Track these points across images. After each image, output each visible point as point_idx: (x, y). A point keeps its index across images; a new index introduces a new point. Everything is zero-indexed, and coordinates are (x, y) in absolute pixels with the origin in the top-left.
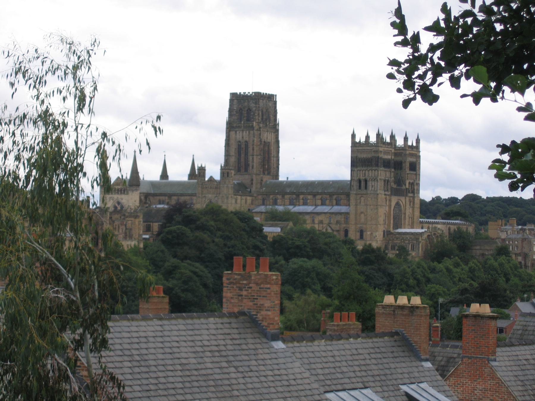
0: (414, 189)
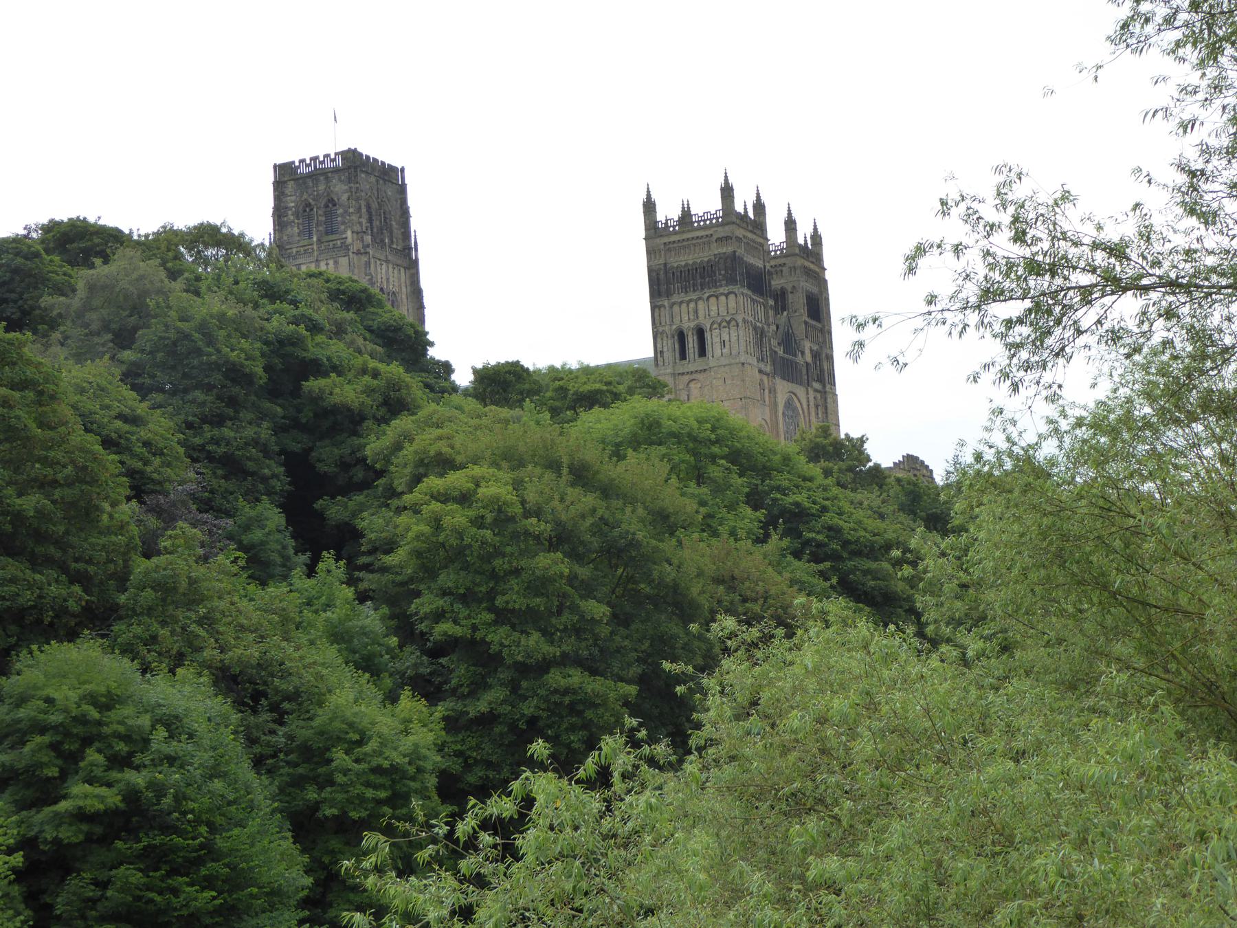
0: (822, 371)
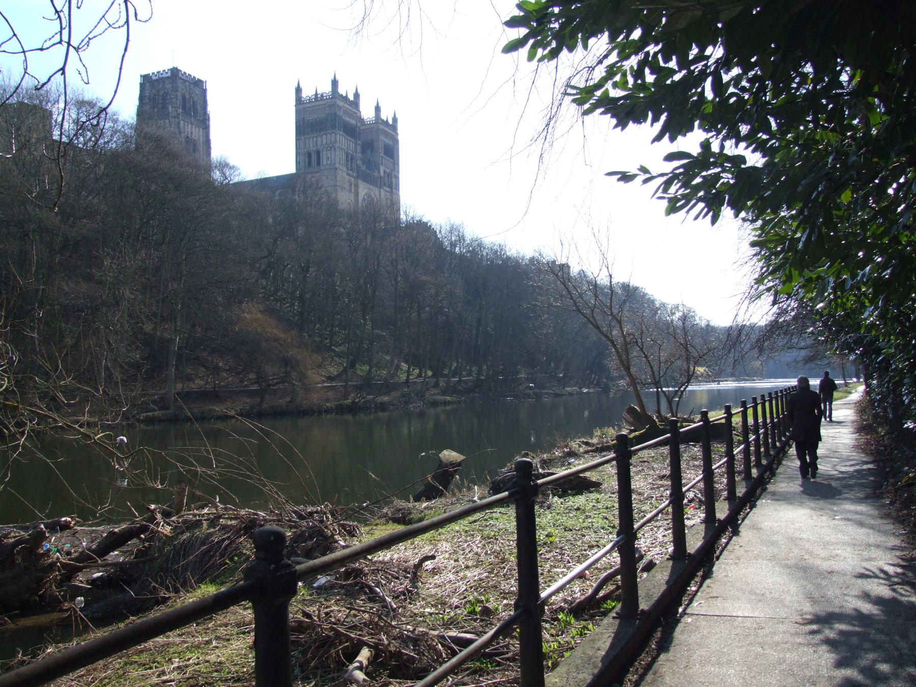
0: (392, 182)
